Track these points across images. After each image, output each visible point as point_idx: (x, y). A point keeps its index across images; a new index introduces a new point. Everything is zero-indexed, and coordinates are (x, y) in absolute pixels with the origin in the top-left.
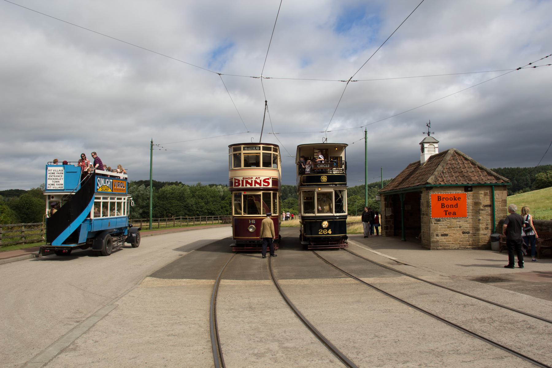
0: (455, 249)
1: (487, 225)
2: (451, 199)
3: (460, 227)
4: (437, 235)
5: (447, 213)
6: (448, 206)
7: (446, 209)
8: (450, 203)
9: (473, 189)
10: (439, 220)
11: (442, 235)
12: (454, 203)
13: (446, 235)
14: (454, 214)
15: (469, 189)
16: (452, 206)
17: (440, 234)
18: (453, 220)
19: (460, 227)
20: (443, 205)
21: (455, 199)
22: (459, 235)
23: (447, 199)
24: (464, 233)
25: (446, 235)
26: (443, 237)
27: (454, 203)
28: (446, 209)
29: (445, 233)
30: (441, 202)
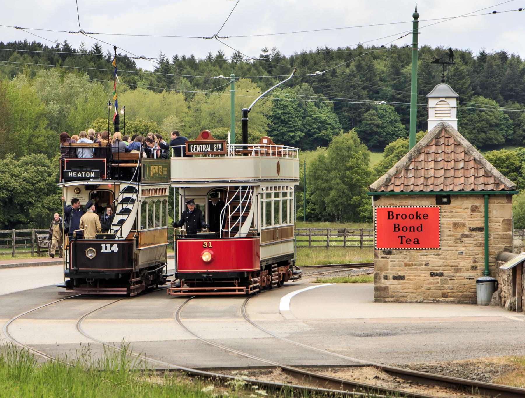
0: (417, 302)
1: (475, 262)
2: (411, 217)
3: (427, 265)
4: (386, 278)
5: (404, 240)
7: (401, 233)
8: (408, 223)
9: (452, 201)
10: (389, 253)
11: (395, 278)
12: (416, 223)
13: (402, 278)
14: (417, 242)
15: (445, 200)
16: (412, 229)
17: (391, 277)
18: (414, 253)
19: (427, 265)
20: (396, 228)
21: (418, 217)
22: (423, 278)
23: (404, 216)
24: (433, 275)
25: (402, 278)
26: (396, 282)
27: (416, 223)
28: (401, 233)
29: (400, 274)
30: (395, 221)
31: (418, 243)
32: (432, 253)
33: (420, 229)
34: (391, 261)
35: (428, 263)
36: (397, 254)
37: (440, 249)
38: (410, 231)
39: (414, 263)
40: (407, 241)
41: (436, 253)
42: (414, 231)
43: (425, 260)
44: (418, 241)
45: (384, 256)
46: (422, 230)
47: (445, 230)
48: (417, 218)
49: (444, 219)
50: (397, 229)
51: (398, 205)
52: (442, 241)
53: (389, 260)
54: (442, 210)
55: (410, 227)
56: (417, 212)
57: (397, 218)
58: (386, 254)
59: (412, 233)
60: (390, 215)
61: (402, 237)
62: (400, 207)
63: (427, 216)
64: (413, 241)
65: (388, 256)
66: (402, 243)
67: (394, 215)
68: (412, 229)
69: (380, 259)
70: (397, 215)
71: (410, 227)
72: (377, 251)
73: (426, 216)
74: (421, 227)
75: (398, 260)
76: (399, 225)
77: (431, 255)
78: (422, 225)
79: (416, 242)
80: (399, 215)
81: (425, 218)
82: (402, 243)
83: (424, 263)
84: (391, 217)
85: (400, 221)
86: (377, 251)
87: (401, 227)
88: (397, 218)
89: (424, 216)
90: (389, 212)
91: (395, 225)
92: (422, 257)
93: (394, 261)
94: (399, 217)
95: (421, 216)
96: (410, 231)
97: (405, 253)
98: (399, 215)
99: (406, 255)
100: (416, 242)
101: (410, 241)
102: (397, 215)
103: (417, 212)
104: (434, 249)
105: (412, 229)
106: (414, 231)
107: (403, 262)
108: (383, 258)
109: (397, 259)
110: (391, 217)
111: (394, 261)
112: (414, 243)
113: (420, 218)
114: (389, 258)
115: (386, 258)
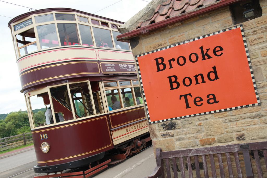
6: (187, 81)
8: (191, 69)
10: (172, 126)
12: (203, 67)
14: (212, 99)
20: (173, 82)
21: (205, 56)
23: (181, 61)
27: (203, 67)
28: (183, 90)
30: (168, 72)
31: (216, 102)
32: (246, 115)
33: (212, 76)
34: (178, 140)
35: (243, 135)
36: (185, 126)
37: (259, 104)
38: (197, 83)
39: (216, 138)
40: (195, 102)
41: (254, 114)
42: (203, 81)
43: (236, 129)
44: (214, 98)
45: (165, 132)
46: (217, 78)
47: (261, 67)
48: (204, 59)
49: (255, 47)
50: (175, 85)
51: (168, 44)
52: (260, 91)
53: (174, 138)
54: (246, 31)
55: (196, 77)
56: (201, 48)
57: (171, 67)
58: (168, 129)
59: (201, 85)
60: (160, 64)
61: (185, 96)
62: (172, 46)
63: (221, 49)
64: (205, 99)
65: (170, 131)
66: (188, 107)
67: (166, 62)
68: (199, 78)
69: (161, 139)
70: (170, 61)
71: (196, 77)
72: (153, 126)
73: (218, 51)
74: (215, 72)
75: (188, 136)
76: (176, 78)
77: (189, 138)
78: (214, 68)
79: (212, 101)
80: (173, 60)
81: (218, 53)
82: (188, 107)
83: (234, 135)
84: (161, 67)
85: (177, 70)
86: (153, 126)
87: (180, 80)
88: (171, 67)
89: (215, 52)
90: (157, 60)
91: (170, 78)
92: (229, 124)
93: (183, 139)
94: (174, 64)
95: (211, 53)
96: (197, 83)
97: (197, 123)
98: (173, 60)
99: (200, 125)
100: (212, 101)
101: (201, 100)
102: (170, 61)
103: (201, 48)
104: (247, 106)
105: (199, 78)
106: (203, 81)
107: (197, 138)
108: (163, 135)
109: (186, 134)
110: (161, 67)
111: (183, 139)
112: (208, 102)
113: (209, 57)
114: (173, 136)
115: (168, 135)
